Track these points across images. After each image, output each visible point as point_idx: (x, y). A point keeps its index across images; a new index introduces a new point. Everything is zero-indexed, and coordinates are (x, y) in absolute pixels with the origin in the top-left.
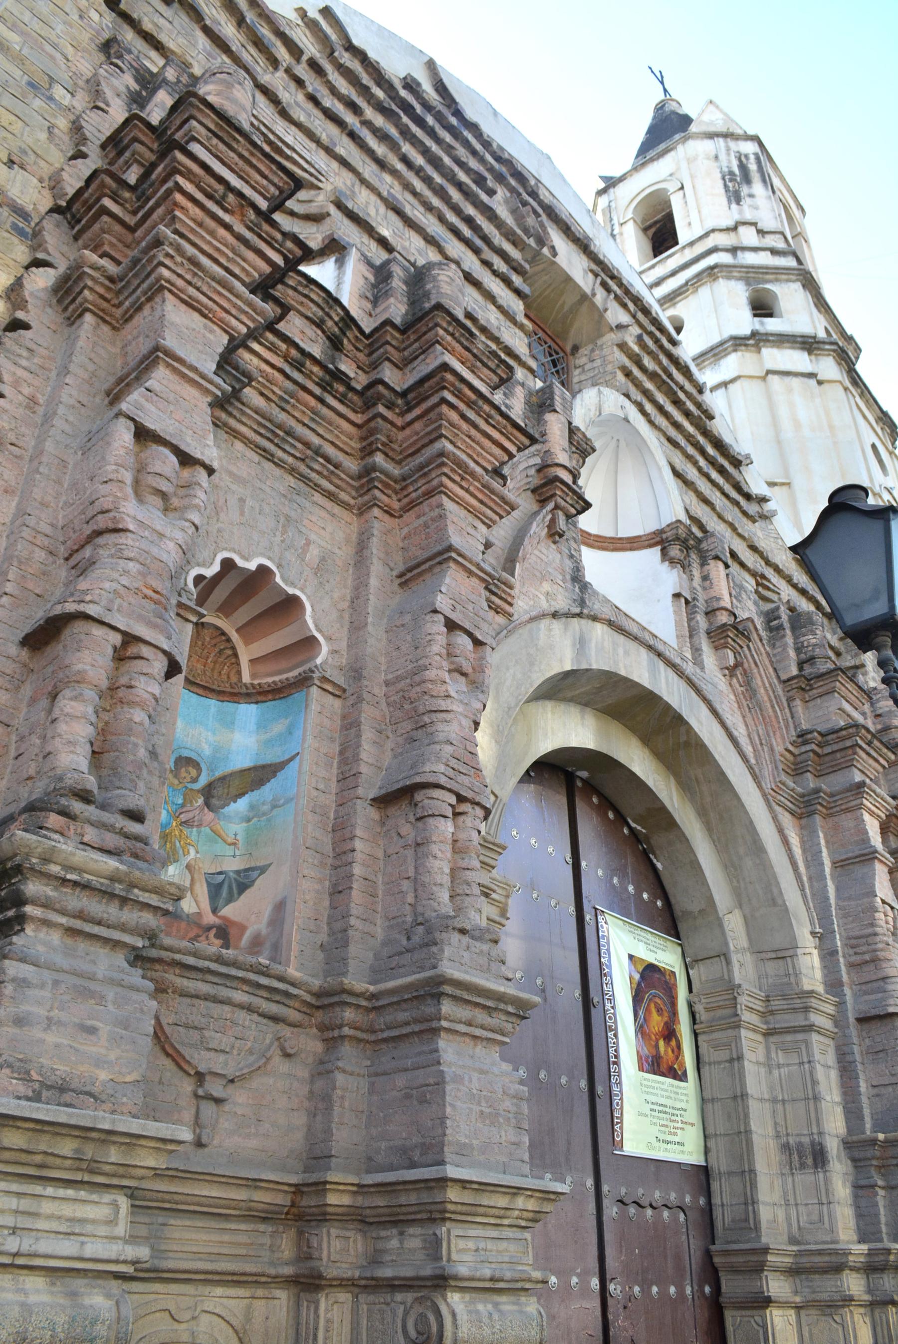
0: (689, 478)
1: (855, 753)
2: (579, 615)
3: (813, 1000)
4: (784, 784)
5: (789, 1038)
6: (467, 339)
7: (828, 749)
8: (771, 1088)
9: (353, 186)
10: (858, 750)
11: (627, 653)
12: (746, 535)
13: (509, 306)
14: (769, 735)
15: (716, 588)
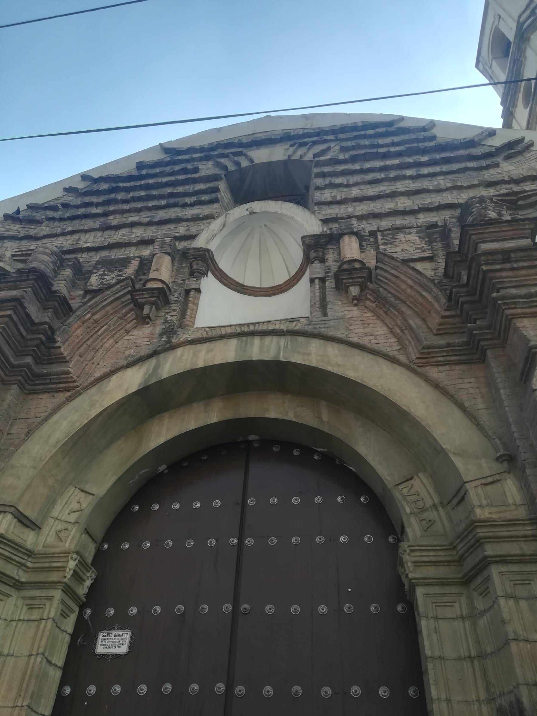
0: (388, 192)
1: (491, 279)
2: (155, 353)
3: (479, 530)
4: (429, 347)
5: (479, 580)
6: (4, 278)
7: (478, 292)
8: (478, 641)
9: (80, 238)
10: (491, 275)
11: (207, 352)
12: (476, 182)
13: (193, 215)
14: (406, 320)
15: (342, 255)
